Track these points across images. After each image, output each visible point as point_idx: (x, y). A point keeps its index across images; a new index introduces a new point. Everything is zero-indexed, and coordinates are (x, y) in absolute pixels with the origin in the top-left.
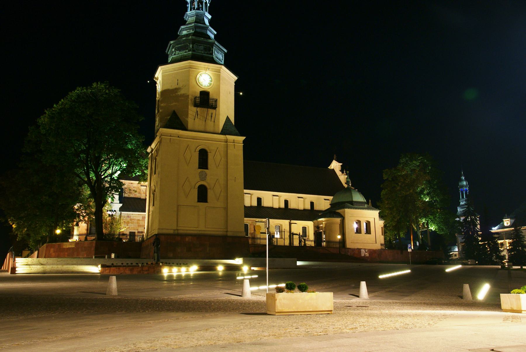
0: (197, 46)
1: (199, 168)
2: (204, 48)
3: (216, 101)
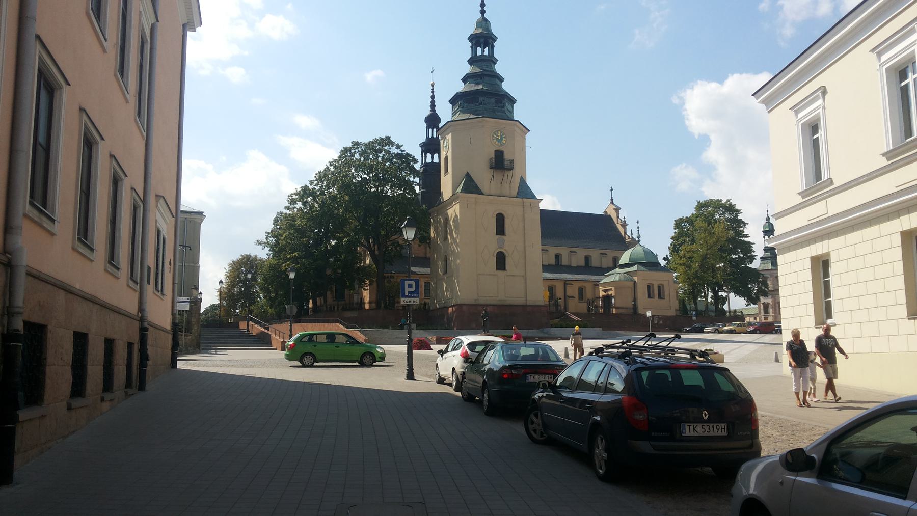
1: (497, 234)
3: (512, 161)
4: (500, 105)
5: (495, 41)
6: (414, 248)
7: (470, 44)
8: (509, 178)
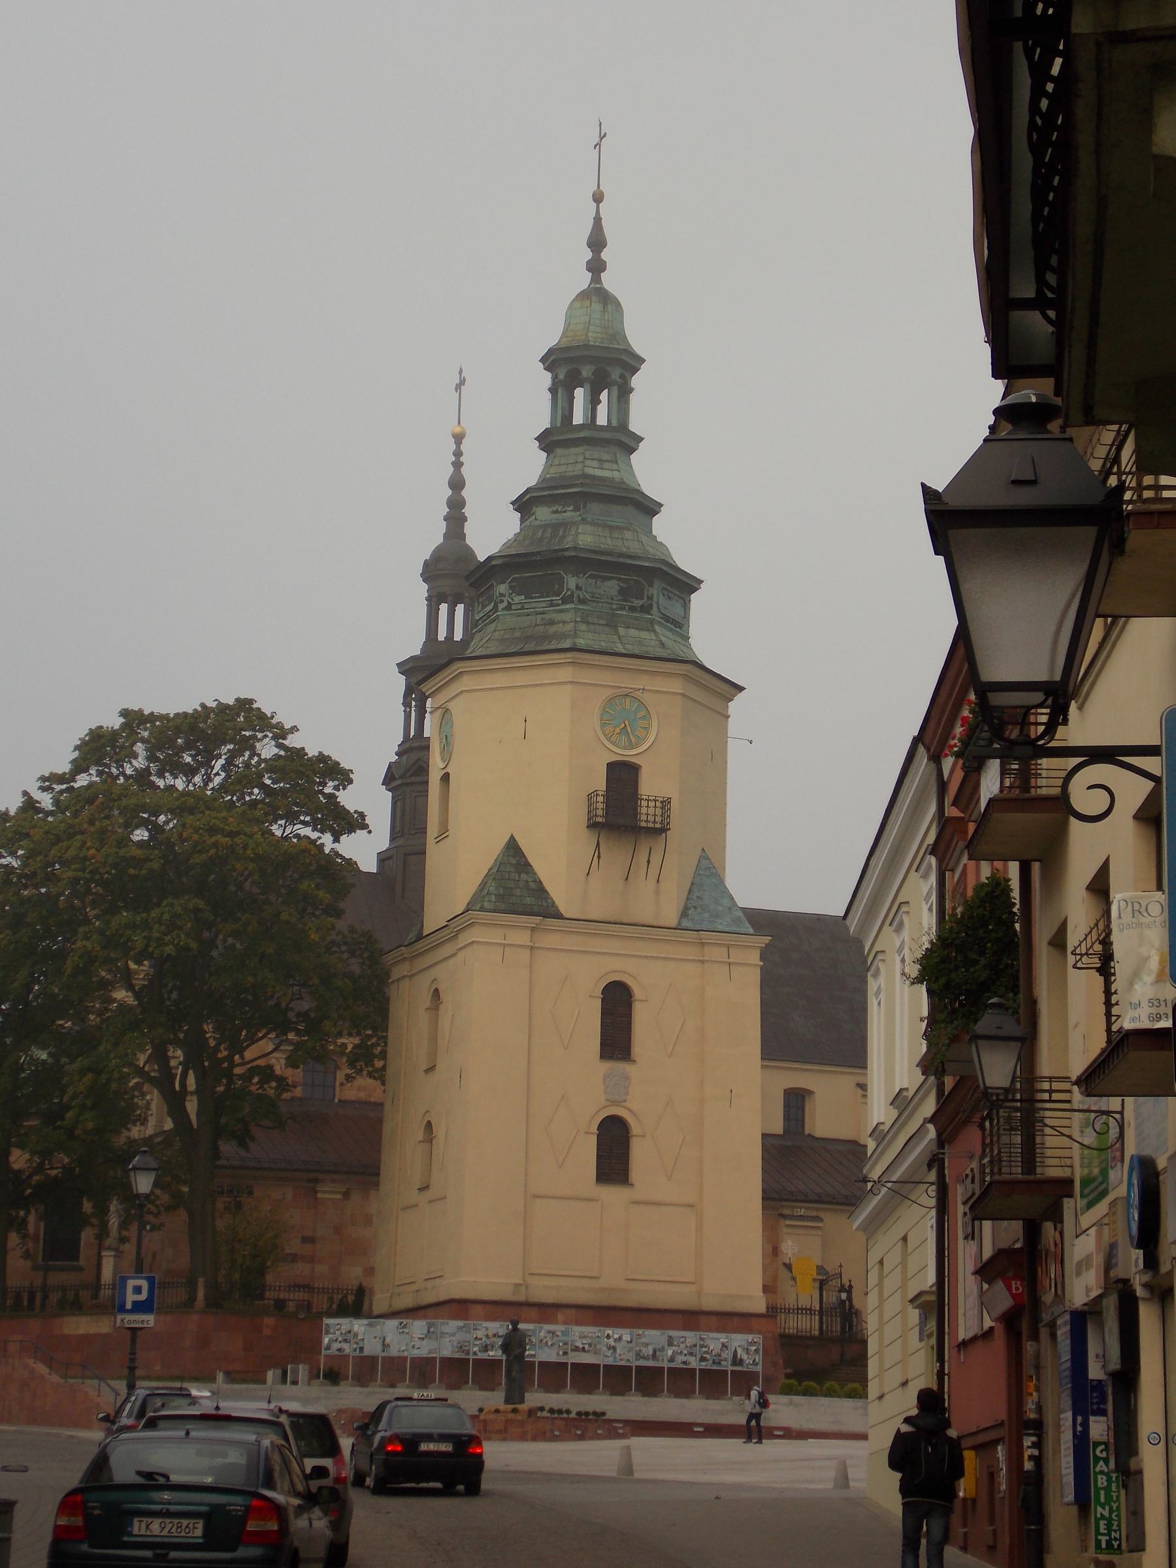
0: (591, 581)
2: (621, 587)
4: (637, 603)
5: (635, 370)
7: (547, 378)
8: (656, 859)
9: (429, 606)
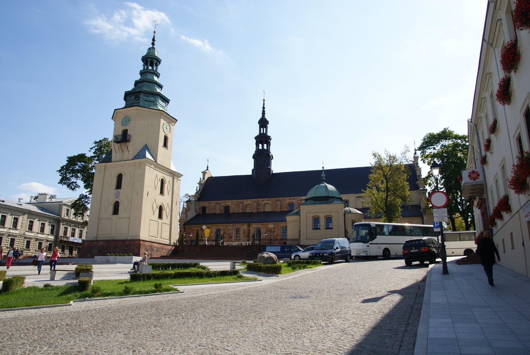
4: (137, 99)
6: (231, 207)
9: (260, 128)
